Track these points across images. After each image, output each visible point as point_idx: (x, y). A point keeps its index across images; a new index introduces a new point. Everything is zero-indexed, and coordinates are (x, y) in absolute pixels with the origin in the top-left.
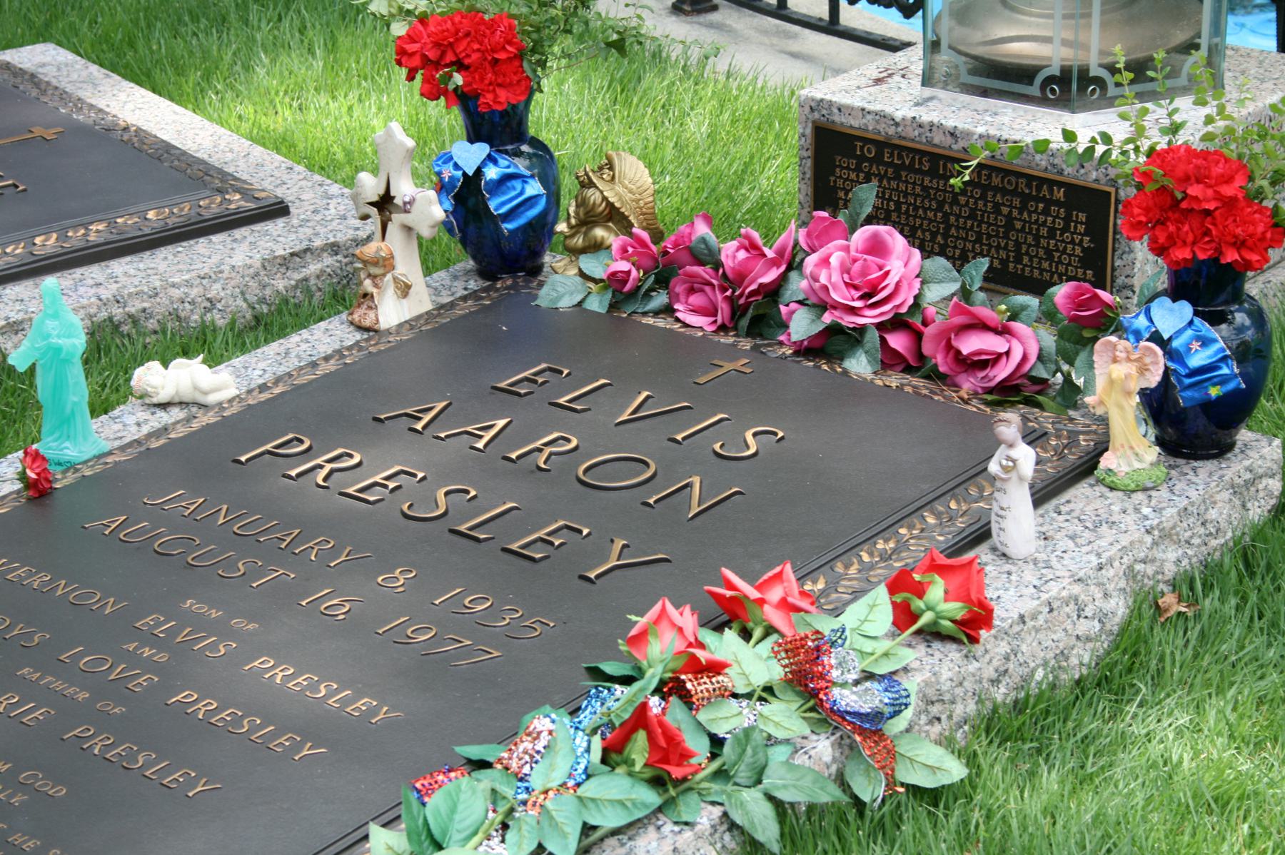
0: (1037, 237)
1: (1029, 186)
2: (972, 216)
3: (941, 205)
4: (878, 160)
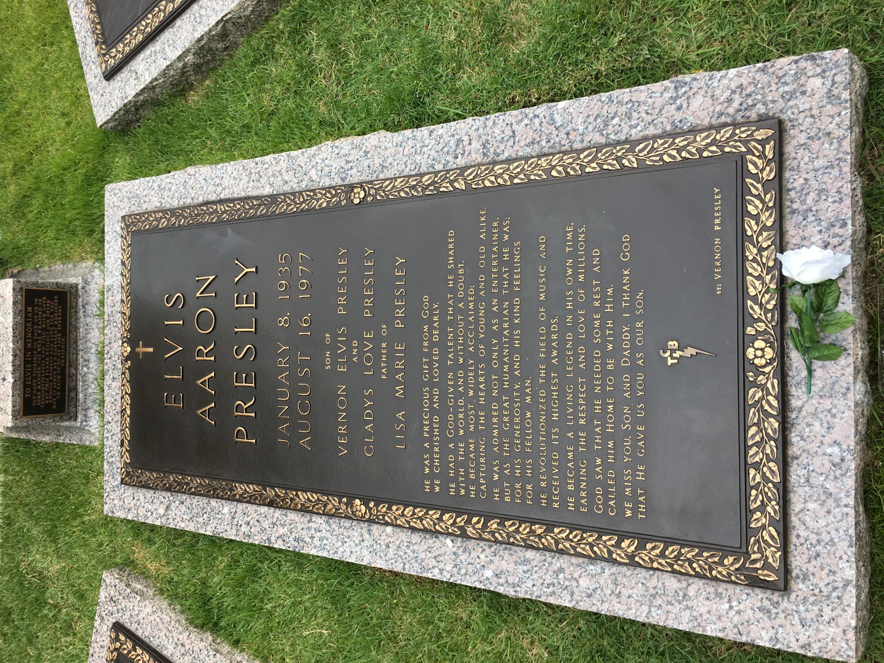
0: (47, 318)
1: (29, 322)
2: (44, 345)
3: (43, 359)
4: (31, 386)
